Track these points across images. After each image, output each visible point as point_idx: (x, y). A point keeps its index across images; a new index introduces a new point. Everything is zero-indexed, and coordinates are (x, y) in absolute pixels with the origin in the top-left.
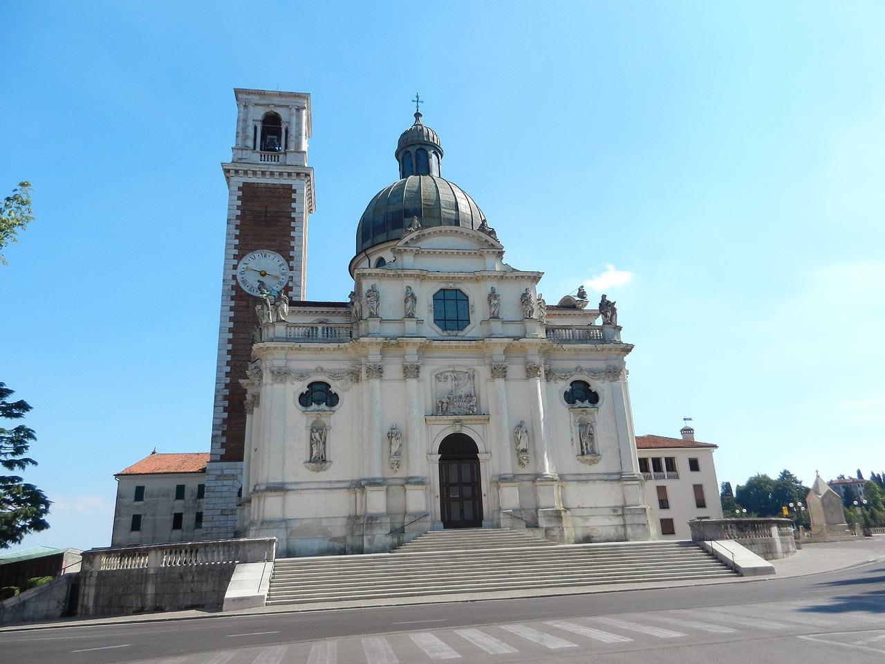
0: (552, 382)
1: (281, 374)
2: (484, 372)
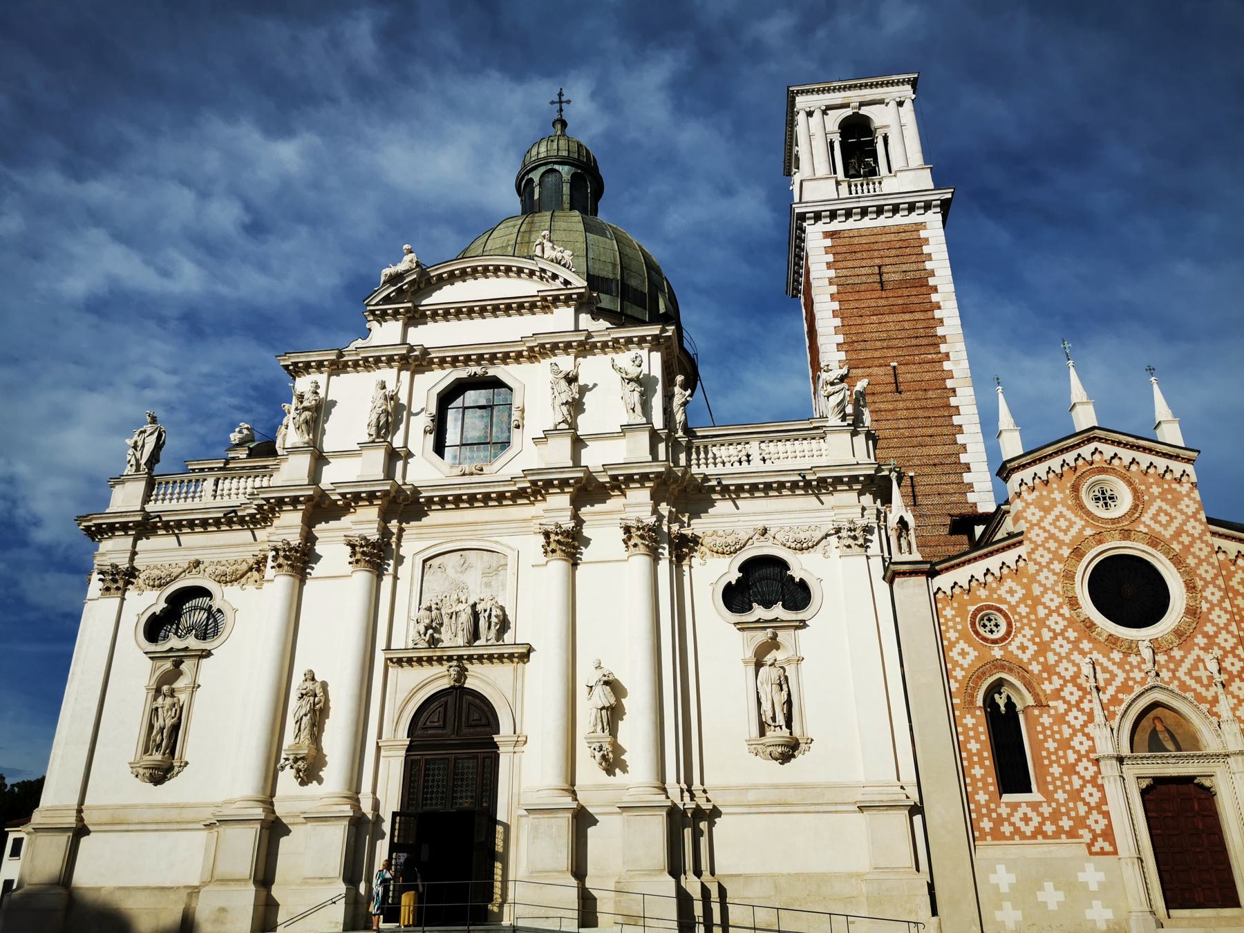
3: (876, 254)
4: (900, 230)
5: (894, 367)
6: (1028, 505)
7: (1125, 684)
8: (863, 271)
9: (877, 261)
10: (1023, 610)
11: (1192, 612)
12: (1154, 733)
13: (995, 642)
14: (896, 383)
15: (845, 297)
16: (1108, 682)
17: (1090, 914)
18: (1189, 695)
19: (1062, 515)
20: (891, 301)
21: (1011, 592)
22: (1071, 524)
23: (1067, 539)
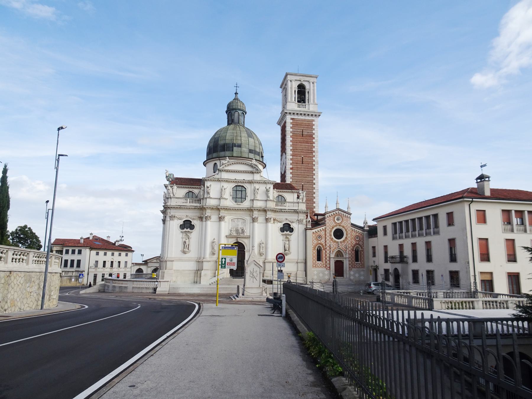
0: (276, 223)
1: (172, 217)
2: (248, 219)
3: (302, 126)
4: (309, 121)
5: (303, 157)
6: (327, 220)
7: (335, 247)
8: (299, 130)
9: (302, 128)
10: (324, 236)
11: (346, 238)
12: (338, 254)
13: (319, 240)
14: (303, 161)
15: (294, 137)
16: (333, 247)
17: (325, 277)
18: (343, 250)
19: (332, 222)
20: (304, 140)
21: (323, 233)
22: (333, 223)
23: (332, 225)
